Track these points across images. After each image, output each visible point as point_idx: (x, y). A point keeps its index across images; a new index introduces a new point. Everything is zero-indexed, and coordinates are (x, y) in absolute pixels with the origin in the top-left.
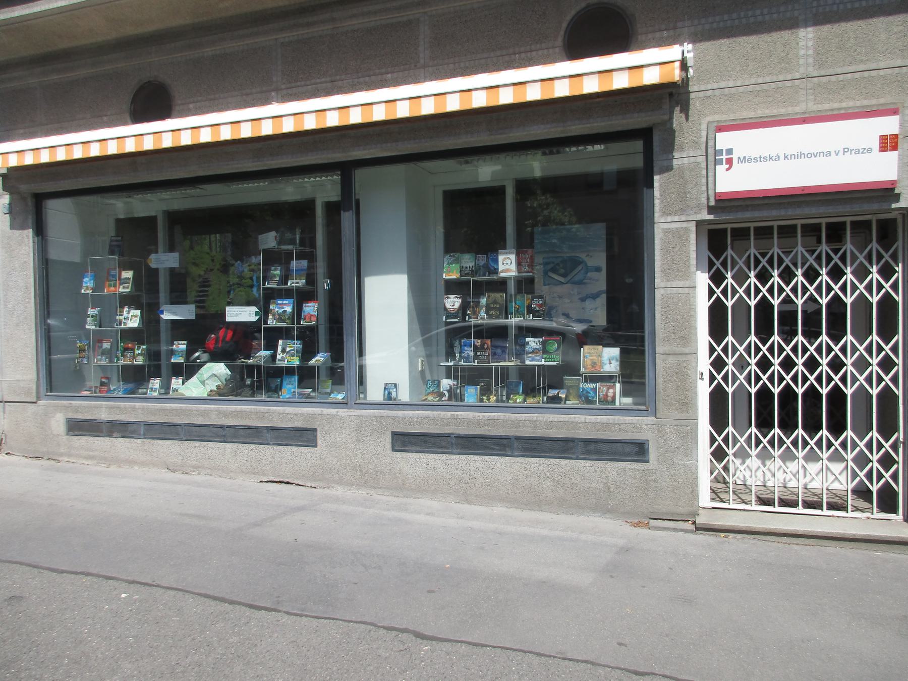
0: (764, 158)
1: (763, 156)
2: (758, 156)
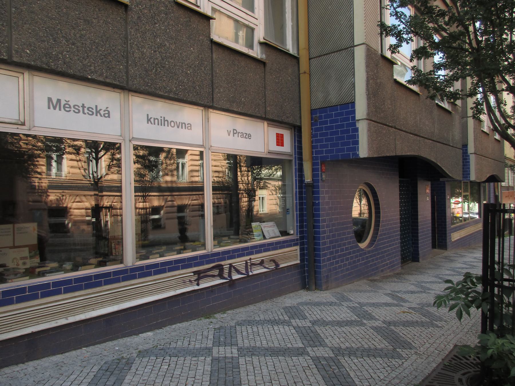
0: (88, 109)
1: (87, 106)
2: (80, 105)
